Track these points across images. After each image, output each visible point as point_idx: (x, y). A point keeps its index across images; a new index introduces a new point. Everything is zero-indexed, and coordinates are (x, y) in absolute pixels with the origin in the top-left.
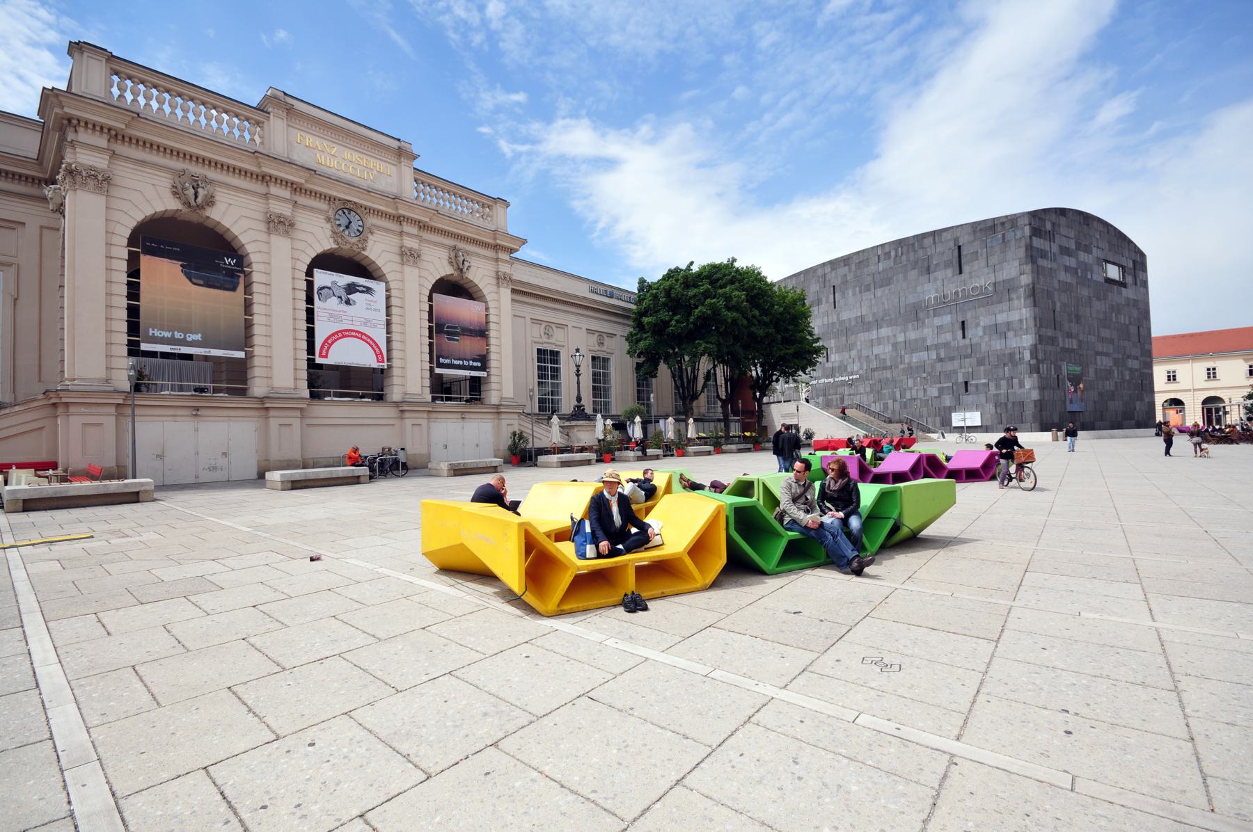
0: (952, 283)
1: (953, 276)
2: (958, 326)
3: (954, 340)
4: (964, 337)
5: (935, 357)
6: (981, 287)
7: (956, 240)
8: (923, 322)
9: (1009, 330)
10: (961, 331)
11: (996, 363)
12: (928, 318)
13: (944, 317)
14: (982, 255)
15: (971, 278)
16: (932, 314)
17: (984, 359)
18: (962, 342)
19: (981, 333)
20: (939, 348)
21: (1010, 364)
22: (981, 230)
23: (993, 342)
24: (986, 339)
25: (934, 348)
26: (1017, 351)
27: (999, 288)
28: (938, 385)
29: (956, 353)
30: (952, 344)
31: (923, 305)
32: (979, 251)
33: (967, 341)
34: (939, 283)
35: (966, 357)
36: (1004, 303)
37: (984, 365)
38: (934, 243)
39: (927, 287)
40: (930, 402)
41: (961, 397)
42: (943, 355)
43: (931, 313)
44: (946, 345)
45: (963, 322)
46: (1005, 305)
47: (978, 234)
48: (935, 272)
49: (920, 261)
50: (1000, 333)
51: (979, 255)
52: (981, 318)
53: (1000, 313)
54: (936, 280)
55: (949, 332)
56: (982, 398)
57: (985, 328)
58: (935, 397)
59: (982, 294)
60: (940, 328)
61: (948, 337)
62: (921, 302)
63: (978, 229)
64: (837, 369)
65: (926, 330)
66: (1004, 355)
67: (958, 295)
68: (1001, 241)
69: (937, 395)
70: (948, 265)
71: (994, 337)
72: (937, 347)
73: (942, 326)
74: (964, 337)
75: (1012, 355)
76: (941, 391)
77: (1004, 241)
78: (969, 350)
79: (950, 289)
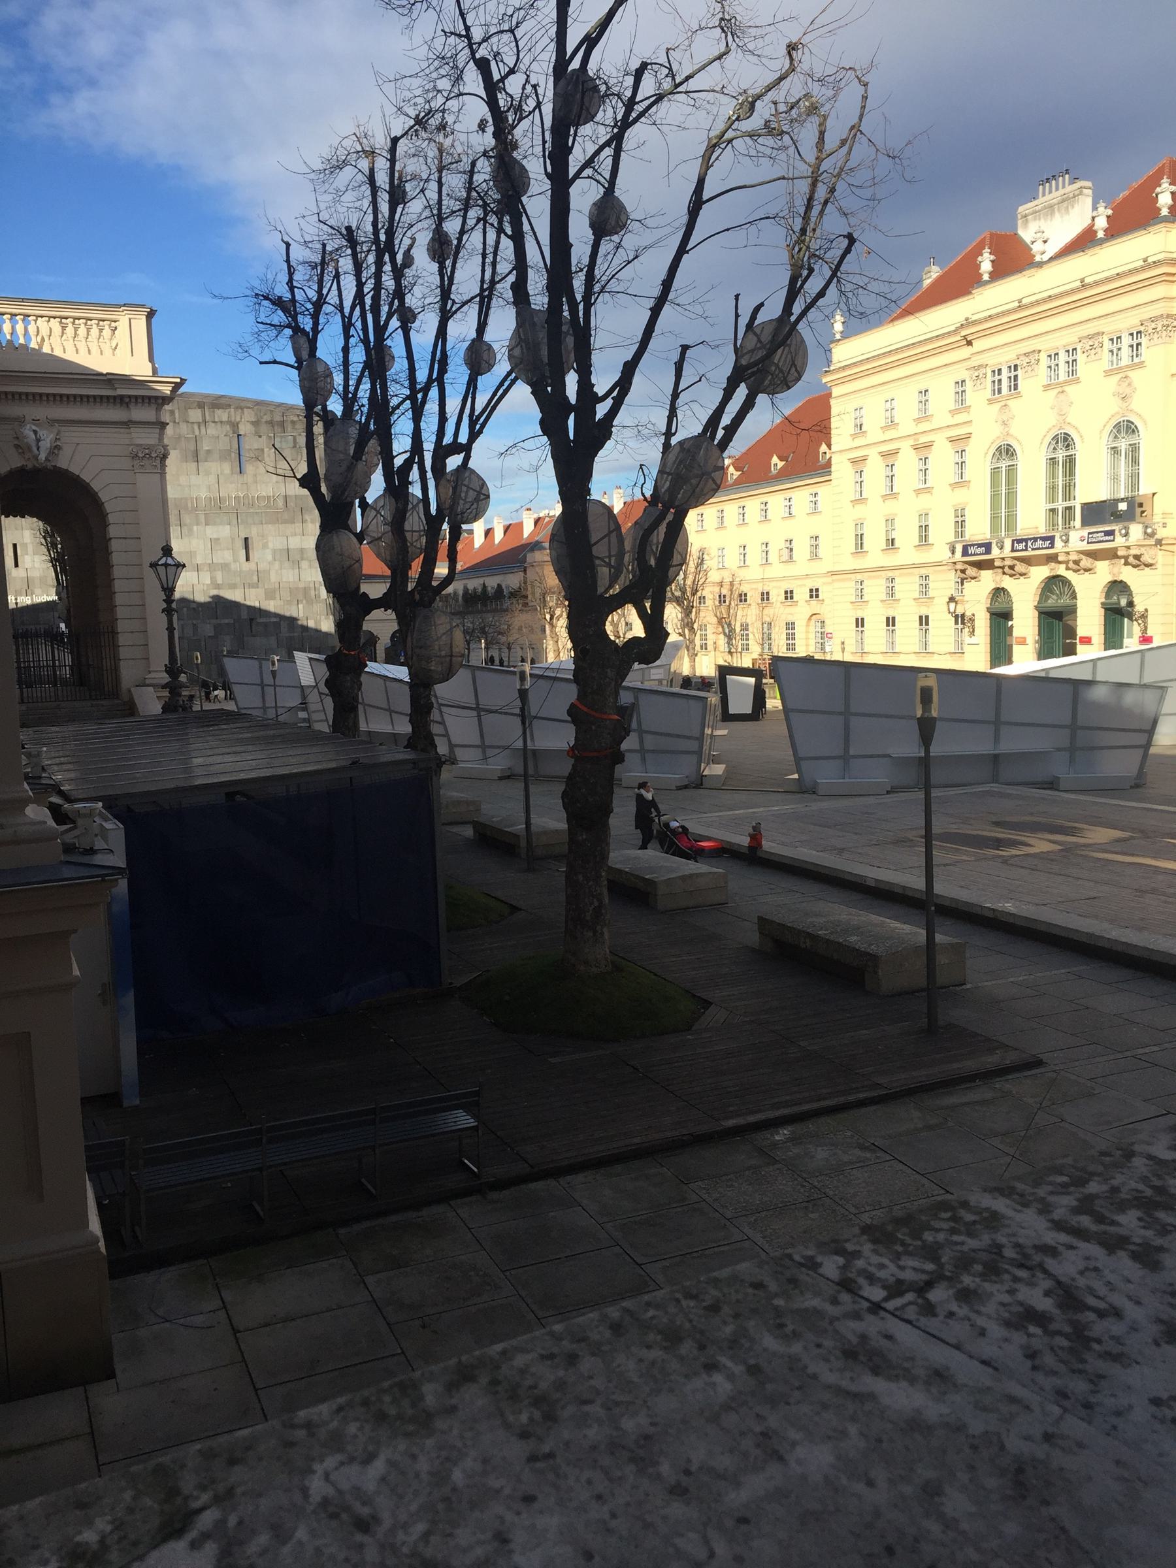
0: (231, 483)
1: (232, 474)
2: (240, 544)
3: (235, 561)
4: (248, 559)
5: (208, 581)
6: (269, 497)
7: (235, 426)
8: (191, 531)
9: (302, 559)
10: (244, 551)
11: (289, 599)
12: (197, 524)
13: (221, 527)
14: (269, 456)
15: (256, 482)
16: (203, 521)
17: (274, 591)
18: (246, 566)
19: (270, 558)
20: (215, 570)
21: (304, 602)
22: (266, 422)
23: (284, 571)
24: (277, 565)
25: (206, 568)
26: (312, 585)
27: (291, 504)
28: (214, 621)
29: (238, 579)
30: (233, 566)
31: (190, 505)
32: (266, 450)
33: (251, 566)
34: (212, 479)
35: (251, 586)
36: (297, 525)
37: (273, 598)
38: (205, 422)
39: (194, 479)
40: (203, 643)
41: (245, 638)
42: (220, 581)
43: (202, 518)
44: (225, 567)
45: (246, 539)
46: (298, 525)
47: (264, 428)
48: (206, 461)
49: (183, 439)
50: (293, 562)
51: (265, 455)
52: (270, 538)
53: (292, 536)
54: (208, 473)
55: (228, 549)
56: (273, 641)
57: (274, 551)
58: (209, 637)
59: (270, 507)
60: (215, 541)
61: (224, 556)
62: (186, 499)
63: (264, 420)
64: (37, 582)
65: (194, 542)
66: (297, 588)
67: (239, 502)
68: (292, 445)
69: (212, 634)
70: (224, 456)
71: (286, 564)
72: (212, 567)
73: (218, 539)
74: (248, 559)
75: (306, 590)
76: (218, 629)
77: (294, 447)
78: (255, 578)
79: (231, 490)
